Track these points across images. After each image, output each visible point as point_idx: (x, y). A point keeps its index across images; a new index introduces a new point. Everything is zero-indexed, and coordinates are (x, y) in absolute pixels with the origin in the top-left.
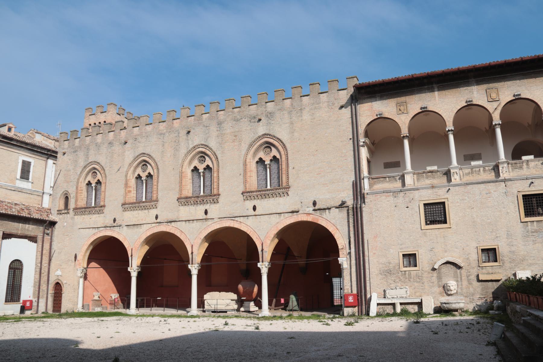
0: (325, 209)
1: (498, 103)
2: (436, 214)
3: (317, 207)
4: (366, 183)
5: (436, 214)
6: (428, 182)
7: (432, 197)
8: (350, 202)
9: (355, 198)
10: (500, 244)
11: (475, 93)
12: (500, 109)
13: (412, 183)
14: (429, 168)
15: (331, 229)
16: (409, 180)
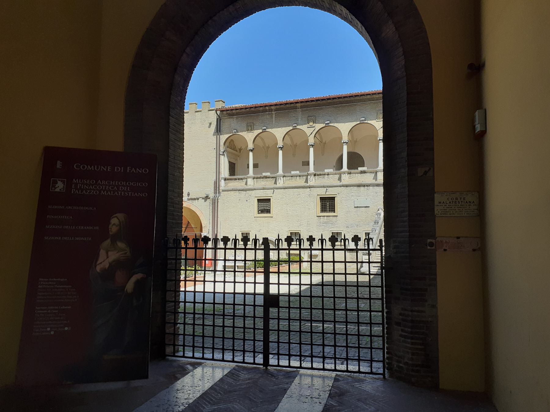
0: (195, 199)
1: (314, 128)
2: (264, 206)
3: (189, 198)
4: (222, 183)
5: (264, 206)
6: (262, 183)
7: (263, 195)
8: (212, 195)
9: (215, 193)
10: (302, 230)
11: (299, 120)
12: (314, 133)
13: (252, 184)
14: (264, 174)
15: (198, 213)
16: (250, 182)
